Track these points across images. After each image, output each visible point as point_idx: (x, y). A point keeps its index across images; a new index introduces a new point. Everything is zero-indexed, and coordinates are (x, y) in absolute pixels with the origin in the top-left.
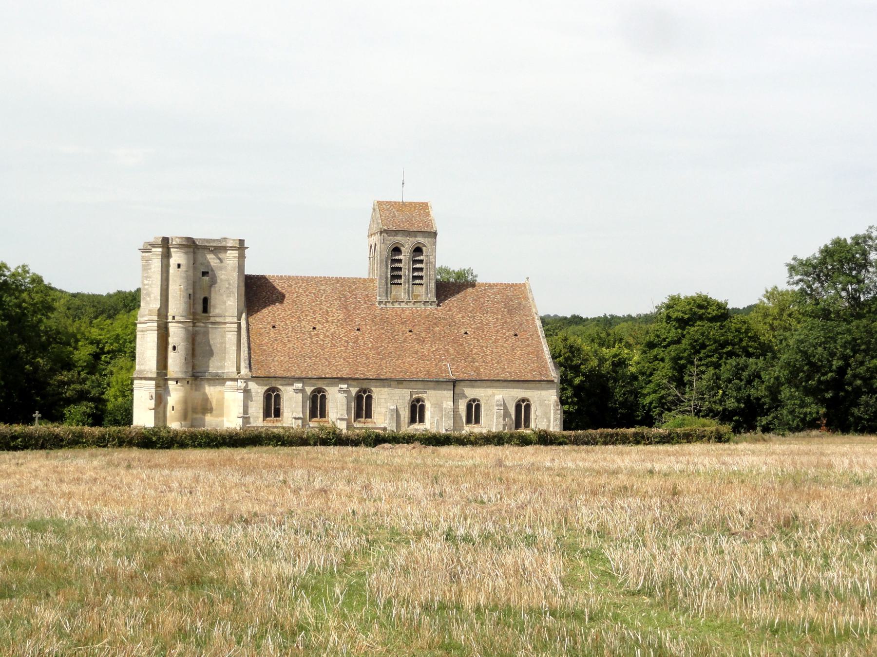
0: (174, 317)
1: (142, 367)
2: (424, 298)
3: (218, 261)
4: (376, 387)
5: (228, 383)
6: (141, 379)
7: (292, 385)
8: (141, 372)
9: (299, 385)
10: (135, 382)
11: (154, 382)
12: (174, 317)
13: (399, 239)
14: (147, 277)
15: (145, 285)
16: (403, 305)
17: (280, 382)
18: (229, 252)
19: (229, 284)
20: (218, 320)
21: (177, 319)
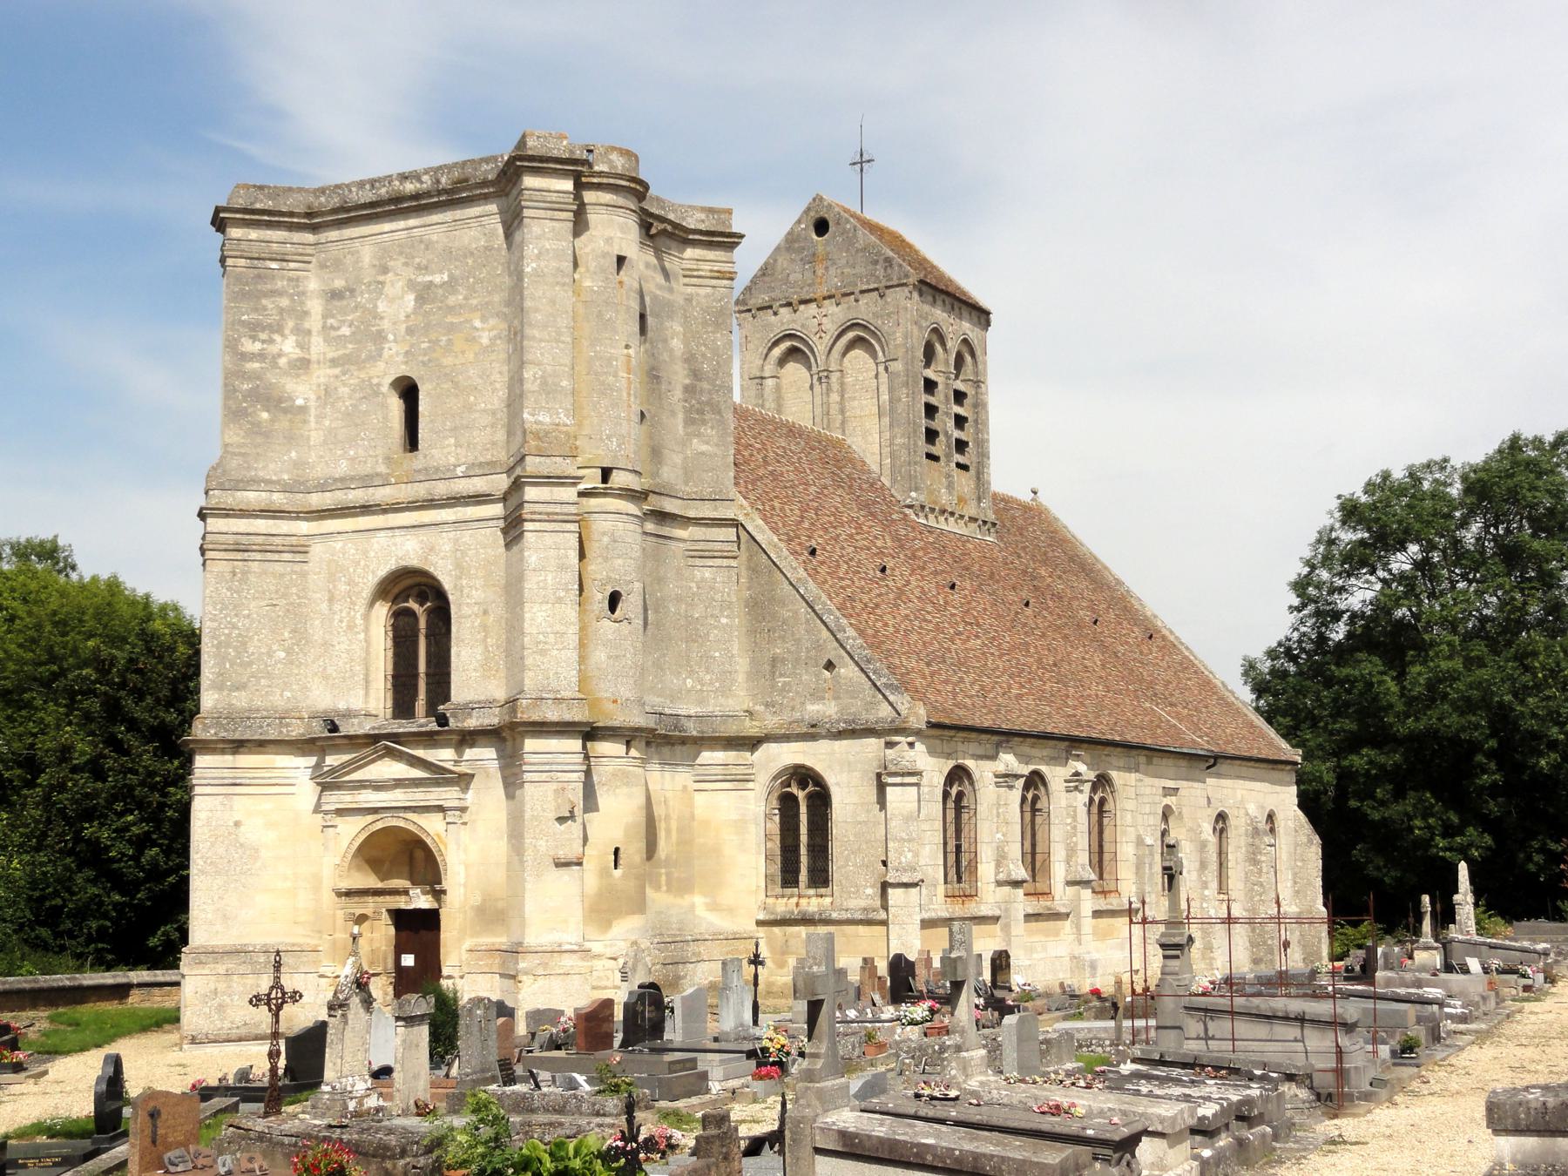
0: (606, 473)
1: (240, 700)
2: (971, 510)
3: (660, 279)
4: (1119, 769)
5: (707, 756)
6: (238, 746)
7: (993, 757)
8: (233, 717)
9: (1008, 761)
10: (201, 761)
11: (575, 744)
12: (606, 473)
13: (939, 315)
14: (254, 329)
15: (245, 357)
16: (952, 526)
17: (973, 748)
18: (690, 252)
19: (696, 374)
20: (670, 506)
21: (619, 479)
